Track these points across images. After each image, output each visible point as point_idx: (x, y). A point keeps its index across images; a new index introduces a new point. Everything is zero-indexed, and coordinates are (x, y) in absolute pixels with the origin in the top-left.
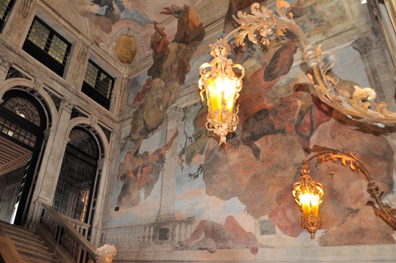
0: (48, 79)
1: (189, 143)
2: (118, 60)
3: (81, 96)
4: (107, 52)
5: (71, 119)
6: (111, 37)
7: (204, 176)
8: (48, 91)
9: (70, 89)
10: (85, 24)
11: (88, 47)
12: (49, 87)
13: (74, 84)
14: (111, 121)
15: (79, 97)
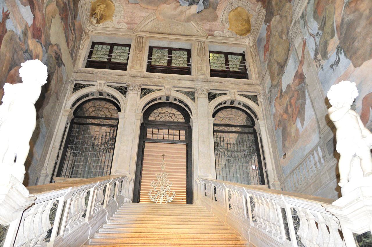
0: (176, 82)
1: (318, 39)
2: (238, 36)
3: (211, 80)
4: (224, 36)
5: (209, 102)
6: (221, 21)
7: (345, 55)
8: (180, 91)
9: (199, 80)
10: (193, 27)
12: (179, 87)
13: (201, 75)
14: (252, 86)
15: (210, 82)
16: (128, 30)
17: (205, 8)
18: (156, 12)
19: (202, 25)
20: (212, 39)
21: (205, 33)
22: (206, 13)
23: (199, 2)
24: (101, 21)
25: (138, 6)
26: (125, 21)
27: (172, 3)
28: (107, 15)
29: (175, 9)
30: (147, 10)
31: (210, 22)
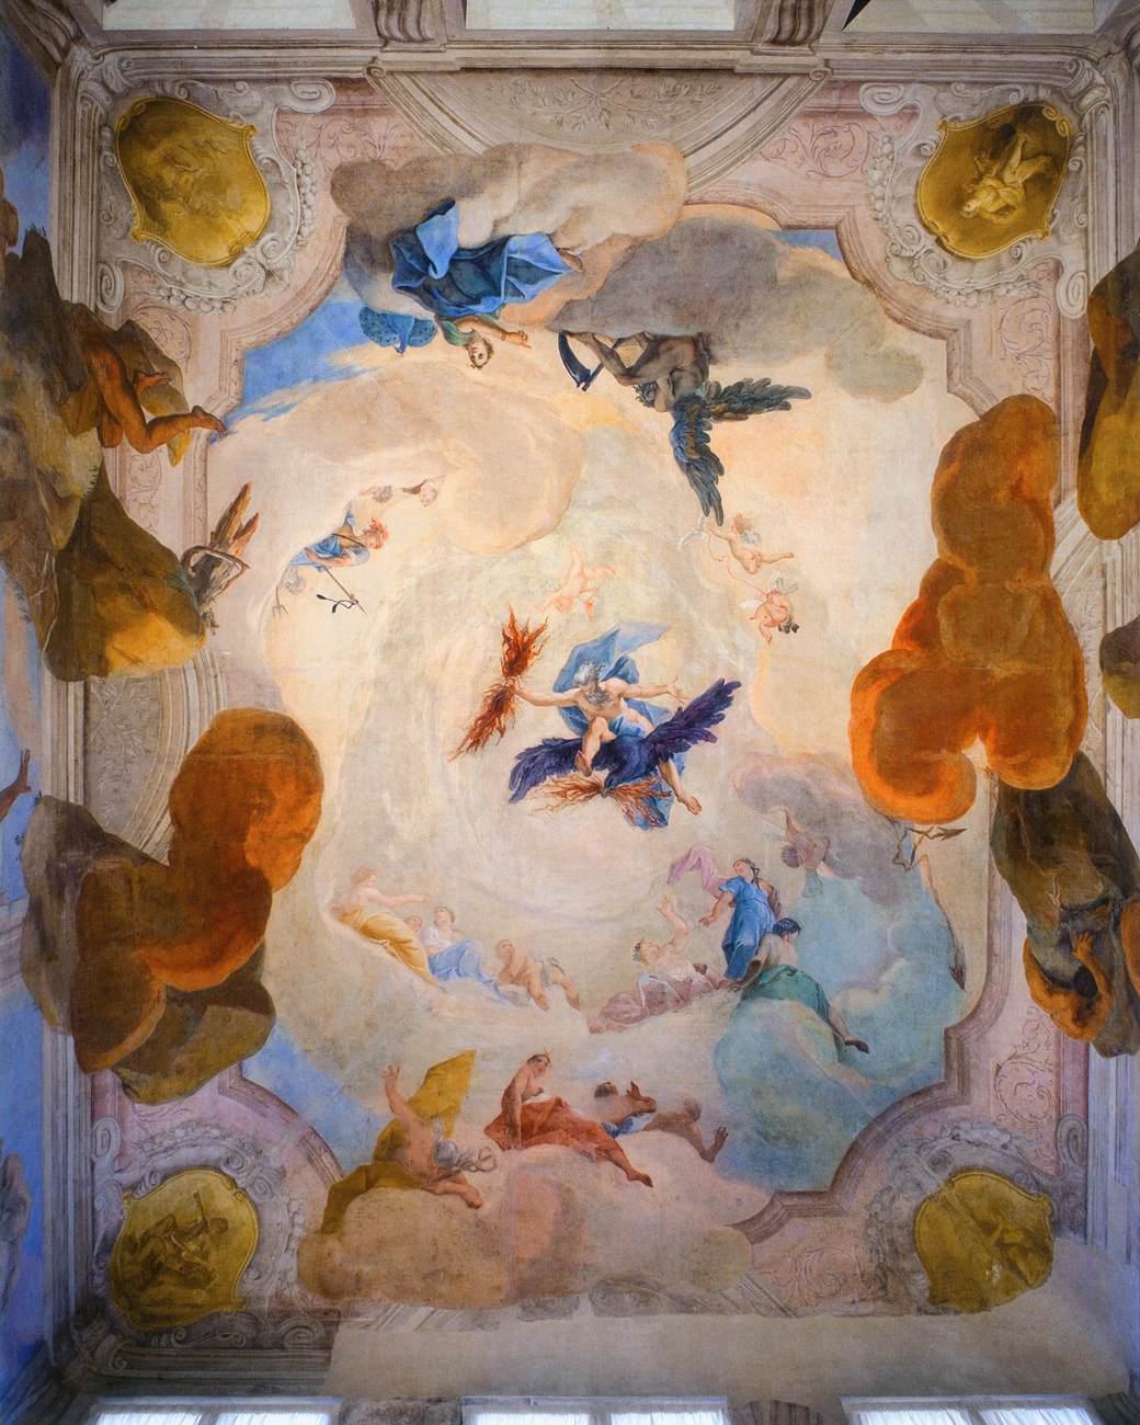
2: (182, 96)
4: (267, 88)
11: (386, 41)
16: (862, 77)
17: (413, 231)
18: (690, 190)
19: (412, 136)
20: (334, 63)
21: (386, 93)
22: (404, 206)
23: (453, 262)
24: (1010, 119)
25: (787, 215)
26: (868, 125)
27: (598, 246)
28: (965, 155)
29: (580, 213)
30: (741, 199)
31: (373, 161)
